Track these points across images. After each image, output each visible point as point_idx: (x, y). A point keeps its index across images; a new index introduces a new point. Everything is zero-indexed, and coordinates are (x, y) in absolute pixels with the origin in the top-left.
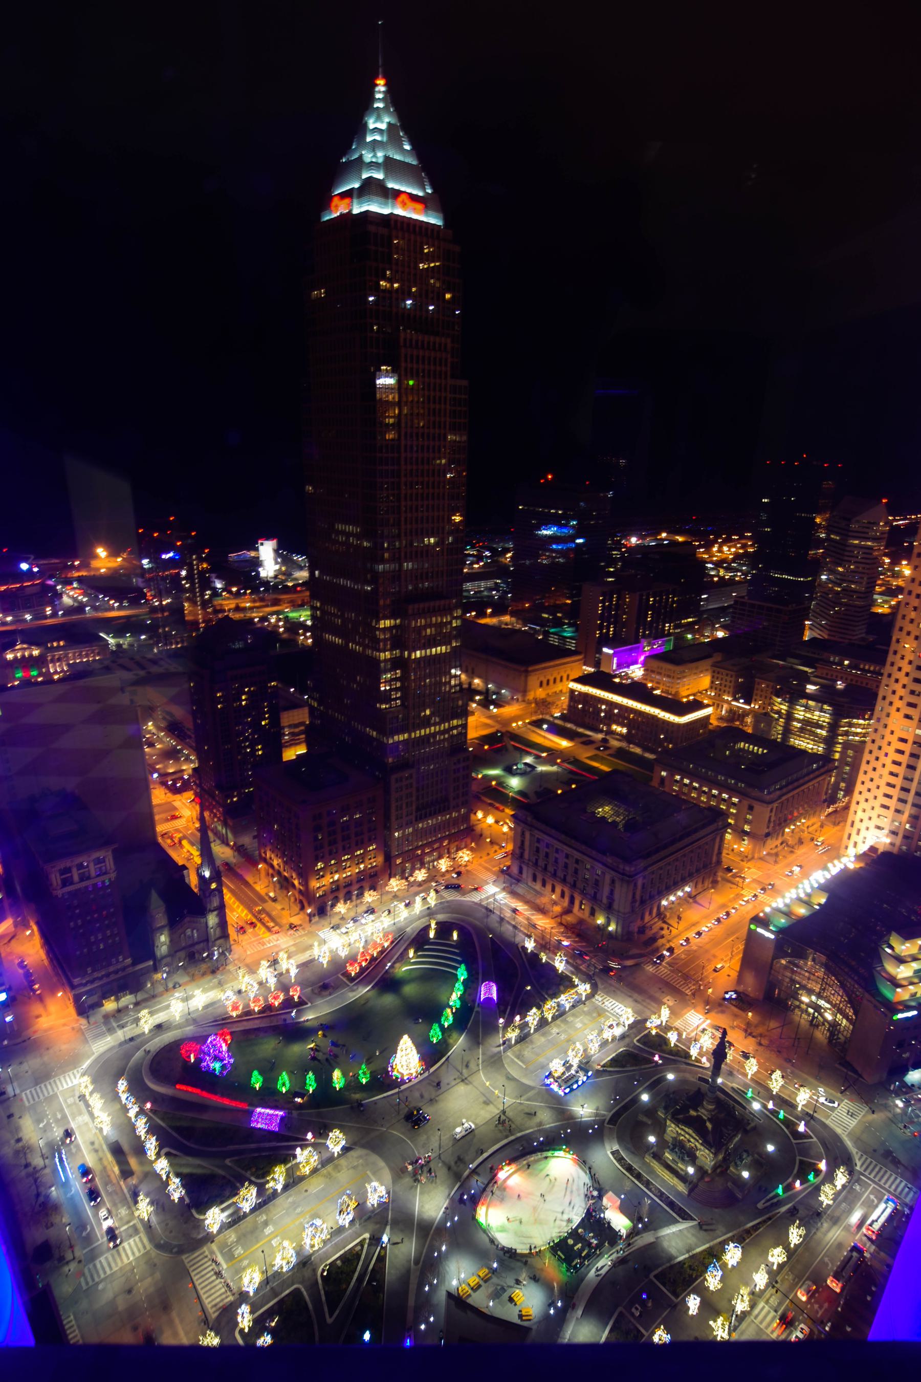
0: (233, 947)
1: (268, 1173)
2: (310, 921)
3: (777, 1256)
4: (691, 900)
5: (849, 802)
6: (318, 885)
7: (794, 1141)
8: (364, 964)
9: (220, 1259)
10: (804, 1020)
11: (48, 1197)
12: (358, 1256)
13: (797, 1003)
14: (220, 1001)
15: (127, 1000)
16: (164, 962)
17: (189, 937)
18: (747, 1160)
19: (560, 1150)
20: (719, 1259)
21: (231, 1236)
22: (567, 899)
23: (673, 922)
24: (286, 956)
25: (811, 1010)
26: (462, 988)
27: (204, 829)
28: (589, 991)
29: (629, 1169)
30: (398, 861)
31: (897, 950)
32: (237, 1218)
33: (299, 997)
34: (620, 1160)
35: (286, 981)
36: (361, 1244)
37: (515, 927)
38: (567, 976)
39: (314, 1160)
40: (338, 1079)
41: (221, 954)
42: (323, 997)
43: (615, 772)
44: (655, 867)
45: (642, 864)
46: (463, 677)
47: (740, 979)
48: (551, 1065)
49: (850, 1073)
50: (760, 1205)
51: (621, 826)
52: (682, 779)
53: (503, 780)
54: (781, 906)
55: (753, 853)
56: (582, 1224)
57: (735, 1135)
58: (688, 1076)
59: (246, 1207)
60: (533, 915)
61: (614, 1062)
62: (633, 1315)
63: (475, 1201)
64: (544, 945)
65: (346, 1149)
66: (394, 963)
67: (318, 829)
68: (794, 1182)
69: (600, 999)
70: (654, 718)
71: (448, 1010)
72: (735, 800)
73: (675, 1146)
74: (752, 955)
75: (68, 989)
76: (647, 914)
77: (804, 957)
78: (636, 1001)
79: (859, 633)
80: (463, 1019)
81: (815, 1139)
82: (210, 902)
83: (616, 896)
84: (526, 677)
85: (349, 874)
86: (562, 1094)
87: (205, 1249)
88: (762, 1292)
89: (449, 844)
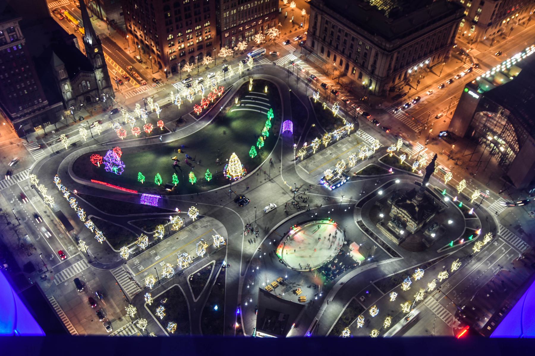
0: (115, 94)
1: (154, 229)
2: (167, 77)
3: (443, 276)
4: (428, 70)
6: (170, 51)
7: (465, 219)
8: (205, 107)
9: (131, 271)
11: (25, 240)
12: (210, 271)
13: (485, 140)
14: (111, 129)
15: (50, 128)
16: (70, 103)
17: (85, 87)
18: (436, 228)
19: (327, 220)
20: (411, 276)
21: (136, 261)
22: (344, 66)
24: (152, 100)
25: (492, 145)
26: (270, 124)
28: (353, 128)
29: (367, 230)
30: (227, 35)
32: (138, 252)
33: (163, 128)
34: (362, 226)
35: (154, 117)
36: (211, 265)
38: (339, 119)
39: (181, 222)
40: (192, 178)
44: (407, 46)
45: (398, 42)
47: (451, 124)
48: (325, 173)
49: (507, 183)
50: (439, 251)
51: (387, 14)
54: (488, 76)
55: (477, 38)
56: (337, 256)
57: (431, 215)
58: (409, 181)
59: (143, 246)
60: (319, 76)
61: (364, 172)
62: (360, 300)
63: (276, 245)
64: (325, 98)
65: (199, 217)
66: (226, 107)
67: (167, 9)
68: (460, 239)
69: (360, 133)
71: (262, 138)
73: (395, 219)
75: (9, 120)
76: (397, 78)
78: (383, 135)
80: (271, 143)
81: (478, 218)
82: (96, 62)
85: (192, 43)
86: (331, 189)
87: (122, 267)
88: (431, 292)
89: (262, 23)
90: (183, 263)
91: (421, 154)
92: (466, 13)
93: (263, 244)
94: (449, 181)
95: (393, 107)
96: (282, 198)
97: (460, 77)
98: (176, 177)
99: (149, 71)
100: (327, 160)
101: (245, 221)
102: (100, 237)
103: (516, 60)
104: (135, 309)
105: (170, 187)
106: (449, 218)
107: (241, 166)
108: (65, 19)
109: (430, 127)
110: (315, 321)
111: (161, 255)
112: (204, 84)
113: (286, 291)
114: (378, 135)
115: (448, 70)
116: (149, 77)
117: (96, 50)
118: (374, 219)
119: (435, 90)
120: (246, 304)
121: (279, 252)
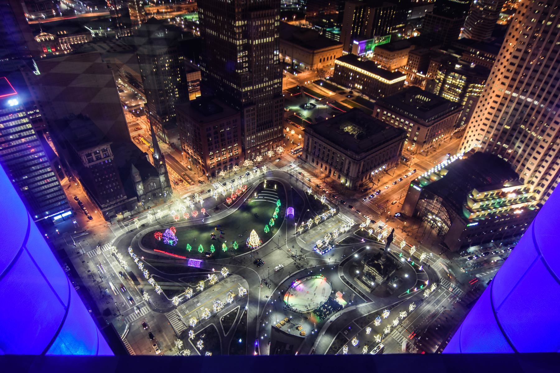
9: (180, 314)
10: (428, 226)
12: (236, 313)
14: (169, 214)
15: (127, 214)
16: (142, 197)
17: (152, 187)
20: (380, 315)
21: (184, 307)
22: (328, 171)
23: (376, 182)
25: (432, 222)
29: (347, 283)
31: (475, 197)
32: (185, 300)
34: (344, 279)
35: (199, 206)
36: (237, 309)
37: (303, 183)
39: (216, 279)
40: (224, 247)
41: (167, 194)
42: (216, 213)
43: (355, 109)
44: (369, 157)
45: (364, 155)
46: (280, 55)
47: (403, 208)
50: (399, 297)
51: (355, 136)
54: (426, 176)
55: (417, 151)
58: (375, 247)
59: (189, 296)
61: (344, 241)
63: (283, 294)
65: (229, 275)
67: (209, 135)
70: (377, 80)
73: (367, 274)
74: (410, 198)
75: (99, 209)
77: (432, 199)
79: (488, 36)
80: (279, 223)
84: (313, 56)
90: (217, 308)
91: (383, 229)
92: (408, 135)
94: (403, 247)
95: (362, 197)
97: (407, 176)
99: (196, 175)
100: (318, 233)
101: (261, 277)
102: (159, 289)
103: (444, 165)
104: (181, 342)
105: (209, 254)
106: (405, 273)
107: (258, 239)
108: (140, 142)
109: (388, 210)
110: (312, 350)
111: (201, 302)
112: (232, 184)
113: (291, 327)
114: (353, 216)
115: (398, 172)
116: (196, 179)
117: (161, 163)
118: (352, 274)
119: (390, 185)
120: (262, 338)
121: (286, 299)
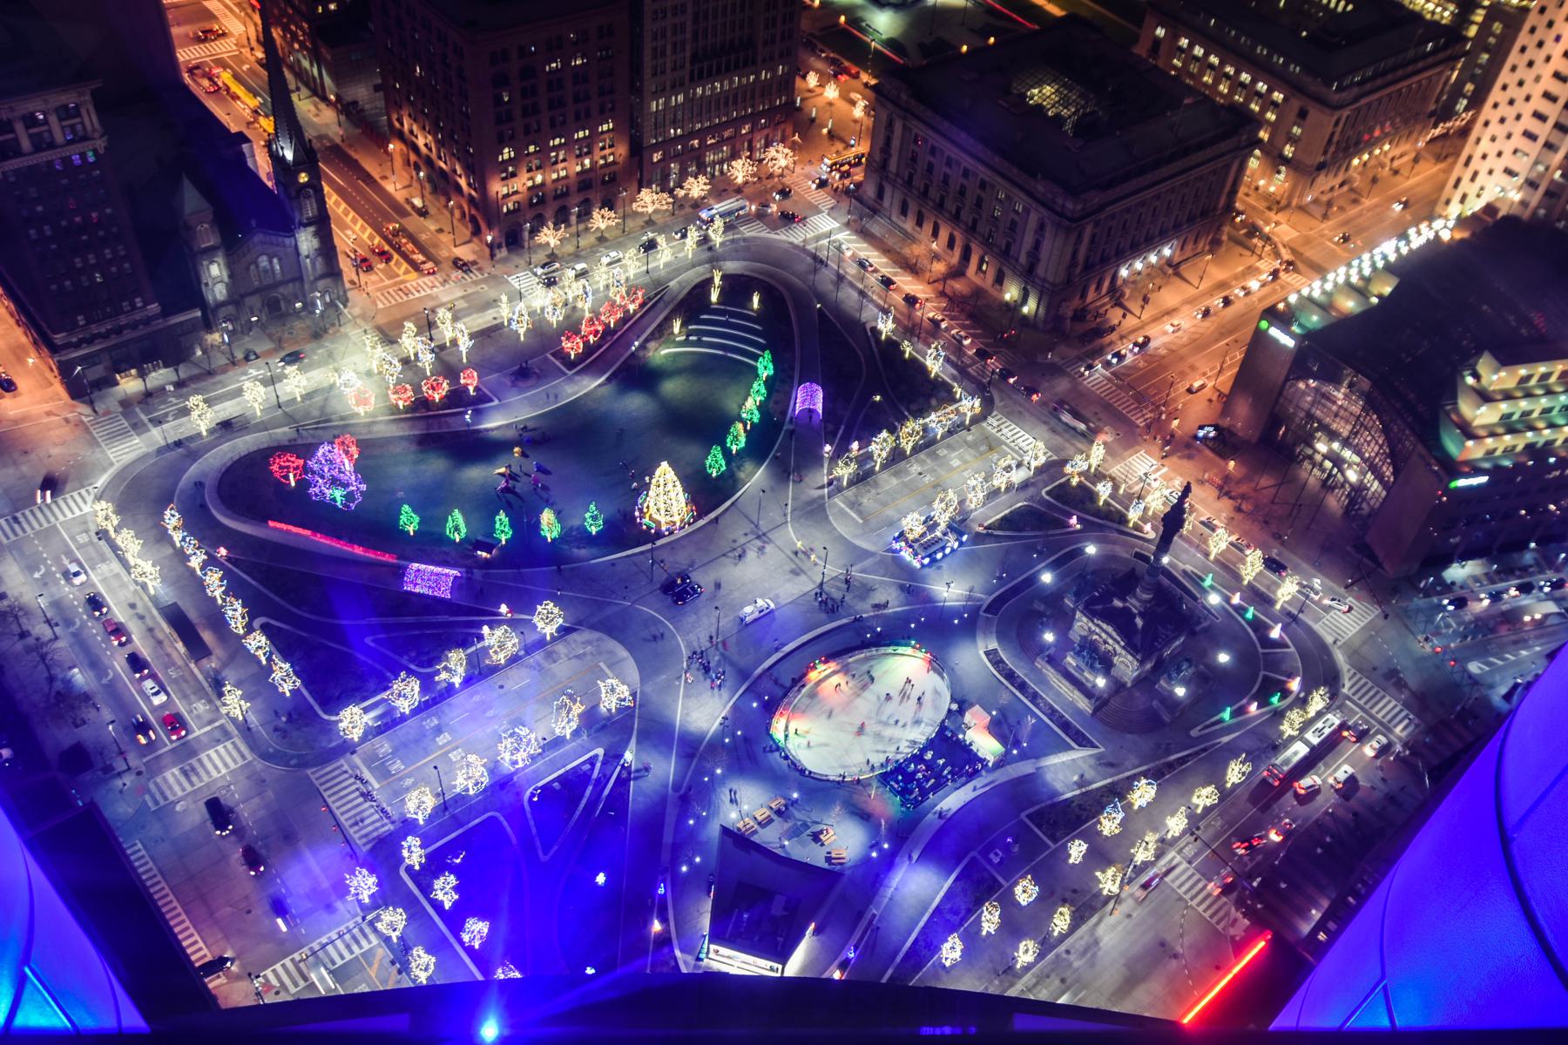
0: (350, 294)
1: (438, 660)
2: (492, 256)
5: (1472, 121)
6: (505, 191)
7: (1260, 650)
8: (592, 339)
9: (367, 775)
10: (1313, 477)
13: (1310, 452)
17: (266, 271)
21: (383, 746)
23: (1134, 306)
24: (449, 315)
25: (1328, 464)
26: (763, 391)
27: (273, 62)
28: (978, 410)
30: (657, 157)
31: (1484, 381)
32: (390, 722)
33: (477, 389)
36: (592, 761)
37: (862, 293)
38: (944, 383)
39: (513, 644)
40: (549, 525)
41: (328, 306)
42: (521, 391)
48: (904, 522)
49: (1365, 560)
52: (1191, 46)
53: (861, 14)
58: (1120, 551)
59: (404, 706)
60: (895, 274)
61: (1006, 522)
64: (911, 329)
65: (564, 631)
66: (647, 340)
69: (995, 424)
71: (740, 426)
72: (1278, 96)
77: (1336, 381)
78: (1054, 431)
80: (763, 442)
81: (1292, 649)
82: (300, 210)
83: (1044, 253)
85: (563, 173)
86: (918, 566)
87: (342, 761)
90: (515, 756)
91: (1146, 480)
93: (735, 708)
94: (1219, 551)
95: (1080, 359)
96: (788, 585)
98: (506, 520)
99: (445, 238)
100: (911, 488)
101: (688, 645)
104: (372, 880)
105: (488, 548)
107: (682, 498)
108: (219, 91)
109: (1173, 415)
111: (452, 731)
114: (1043, 430)
116: (444, 253)
117: (303, 178)
120: (684, 869)
121: (778, 728)
